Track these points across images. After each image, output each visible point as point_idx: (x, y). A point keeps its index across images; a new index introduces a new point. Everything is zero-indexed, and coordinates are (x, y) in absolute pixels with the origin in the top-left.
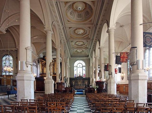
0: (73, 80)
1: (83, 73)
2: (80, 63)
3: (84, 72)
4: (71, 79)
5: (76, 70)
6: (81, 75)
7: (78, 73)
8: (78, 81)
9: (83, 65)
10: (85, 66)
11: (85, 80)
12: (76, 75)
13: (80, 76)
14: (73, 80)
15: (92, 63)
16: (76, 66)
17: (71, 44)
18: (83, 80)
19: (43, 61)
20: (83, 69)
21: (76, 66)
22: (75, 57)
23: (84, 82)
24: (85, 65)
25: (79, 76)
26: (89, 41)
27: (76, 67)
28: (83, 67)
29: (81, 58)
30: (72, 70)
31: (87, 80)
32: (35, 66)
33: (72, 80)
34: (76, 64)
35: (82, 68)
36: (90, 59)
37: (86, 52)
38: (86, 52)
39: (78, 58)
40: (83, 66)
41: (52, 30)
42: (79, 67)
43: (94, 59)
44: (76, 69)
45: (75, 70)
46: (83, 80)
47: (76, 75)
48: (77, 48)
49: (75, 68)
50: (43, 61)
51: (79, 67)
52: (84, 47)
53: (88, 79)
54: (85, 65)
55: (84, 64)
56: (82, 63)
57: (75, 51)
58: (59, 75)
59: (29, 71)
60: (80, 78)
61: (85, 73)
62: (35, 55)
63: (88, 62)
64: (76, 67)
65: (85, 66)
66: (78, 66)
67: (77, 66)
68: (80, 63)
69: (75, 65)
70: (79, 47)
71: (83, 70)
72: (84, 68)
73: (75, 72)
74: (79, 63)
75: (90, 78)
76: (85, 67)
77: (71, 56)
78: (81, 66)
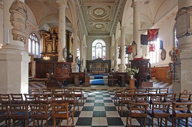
0: (91, 62)
1: (103, 55)
2: (99, 43)
3: (104, 54)
4: (88, 62)
5: (95, 51)
6: (100, 57)
7: (97, 54)
8: (97, 64)
9: (103, 46)
10: (105, 47)
11: (105, 63)
12: (94, 57)
13: (99, 58)
14: (91, 62)
15: (115, 40)
16: (95, 46)
17: (87, 12)
19: (46, 35)
20: (103, 50)
21: (94, 47)
22: (93, 35)
23: (103, 65)
24: (105, 45)
25: (98, 58)
26: (112, 6)
28: (103, 48)
29: (101, 36)
30: (89, 51)
31: (108, 62)
32: (36, 42)
33: (90, 63)
34: (94, 44)
36: (111, 38)
37: (107, 28)
38: (107, 28)
39: (97, 36)
40: (102, 47)
41: (66, 3)
43: (118, 33)
47: (94, 57)
48: (96, 20)
49: (93, 49)
50: (46, 35)
52: (104, 20)
53: (109, 62)
54: (105, 45)
55: (104, 44)
57: (93, 27)
58: (63, 51)
59: (20, 47)
60: (99, 60)
61: (105, 55)
62: (35, 25)
63: (109, 41)
65: (105, 47)
66: (97, 46)
67: (96, 47)
68: (99, 43)
69: (93, 45)
70: (99, 19)
71: (103, 52)
72: (104, 49)
73: (93, 54)
74: (98, 42)
75: (111, 60)
76: (105, 48)
77: (88, 34)
78: (101, 46)
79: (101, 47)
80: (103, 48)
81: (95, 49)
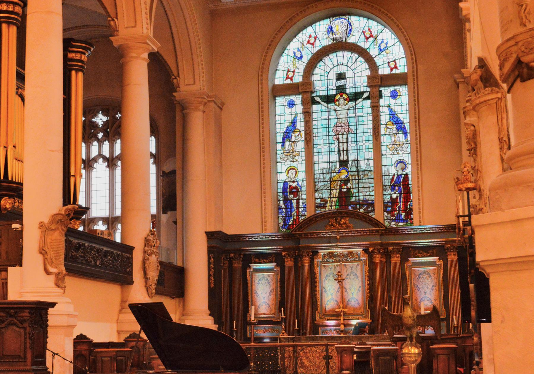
9: (384, 71)
12: (296, 191)
16: (298, 79)
18: (387, 255)
20: (384, 118)
24: (403, 68)
25: (332, 206)
27: (297, 99)
28: (386, 91)
35: (365, 105)
42: (329, 99)
44: (300, 125)
45: (287, 137)
46: (387, 255)
51: (329, 99)
54: (403, 68)
56: (363, 44)
64: (297, 99)
76: (403, 90)
79: (362, 85)
80: (386, 91)
81: (299, 108)
